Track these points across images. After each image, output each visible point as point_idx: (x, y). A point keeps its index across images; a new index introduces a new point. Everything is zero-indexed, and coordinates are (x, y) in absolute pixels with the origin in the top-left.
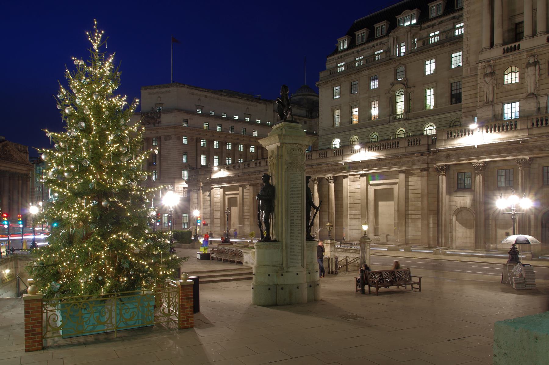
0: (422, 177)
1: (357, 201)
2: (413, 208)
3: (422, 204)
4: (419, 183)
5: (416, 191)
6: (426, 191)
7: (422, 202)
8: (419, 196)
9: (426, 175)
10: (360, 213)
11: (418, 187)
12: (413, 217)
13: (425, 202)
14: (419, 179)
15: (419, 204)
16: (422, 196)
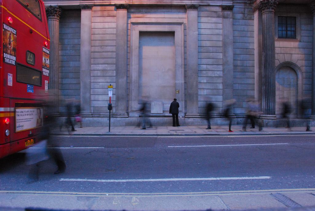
0: (224, 17)
1: (109, 49)
2: (210, 61)
3: (224, 55)
4: (220, 26)
5: (215, 38)
6: (231, 37)
7: (224, 53)
8: (220, 44)
9: (231, 16)
10: (114, 67)
11: (217, 31)
12: (210, 74)
13: (230, 53)
14: (220, 20)
15: (221, 56)
16: (225, 45)
